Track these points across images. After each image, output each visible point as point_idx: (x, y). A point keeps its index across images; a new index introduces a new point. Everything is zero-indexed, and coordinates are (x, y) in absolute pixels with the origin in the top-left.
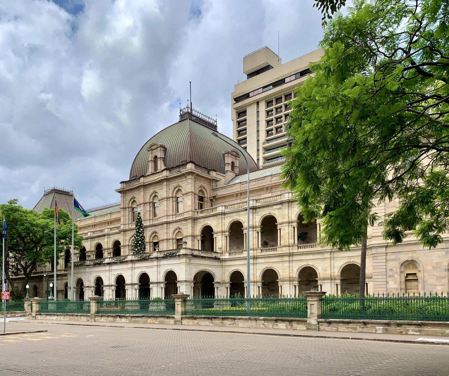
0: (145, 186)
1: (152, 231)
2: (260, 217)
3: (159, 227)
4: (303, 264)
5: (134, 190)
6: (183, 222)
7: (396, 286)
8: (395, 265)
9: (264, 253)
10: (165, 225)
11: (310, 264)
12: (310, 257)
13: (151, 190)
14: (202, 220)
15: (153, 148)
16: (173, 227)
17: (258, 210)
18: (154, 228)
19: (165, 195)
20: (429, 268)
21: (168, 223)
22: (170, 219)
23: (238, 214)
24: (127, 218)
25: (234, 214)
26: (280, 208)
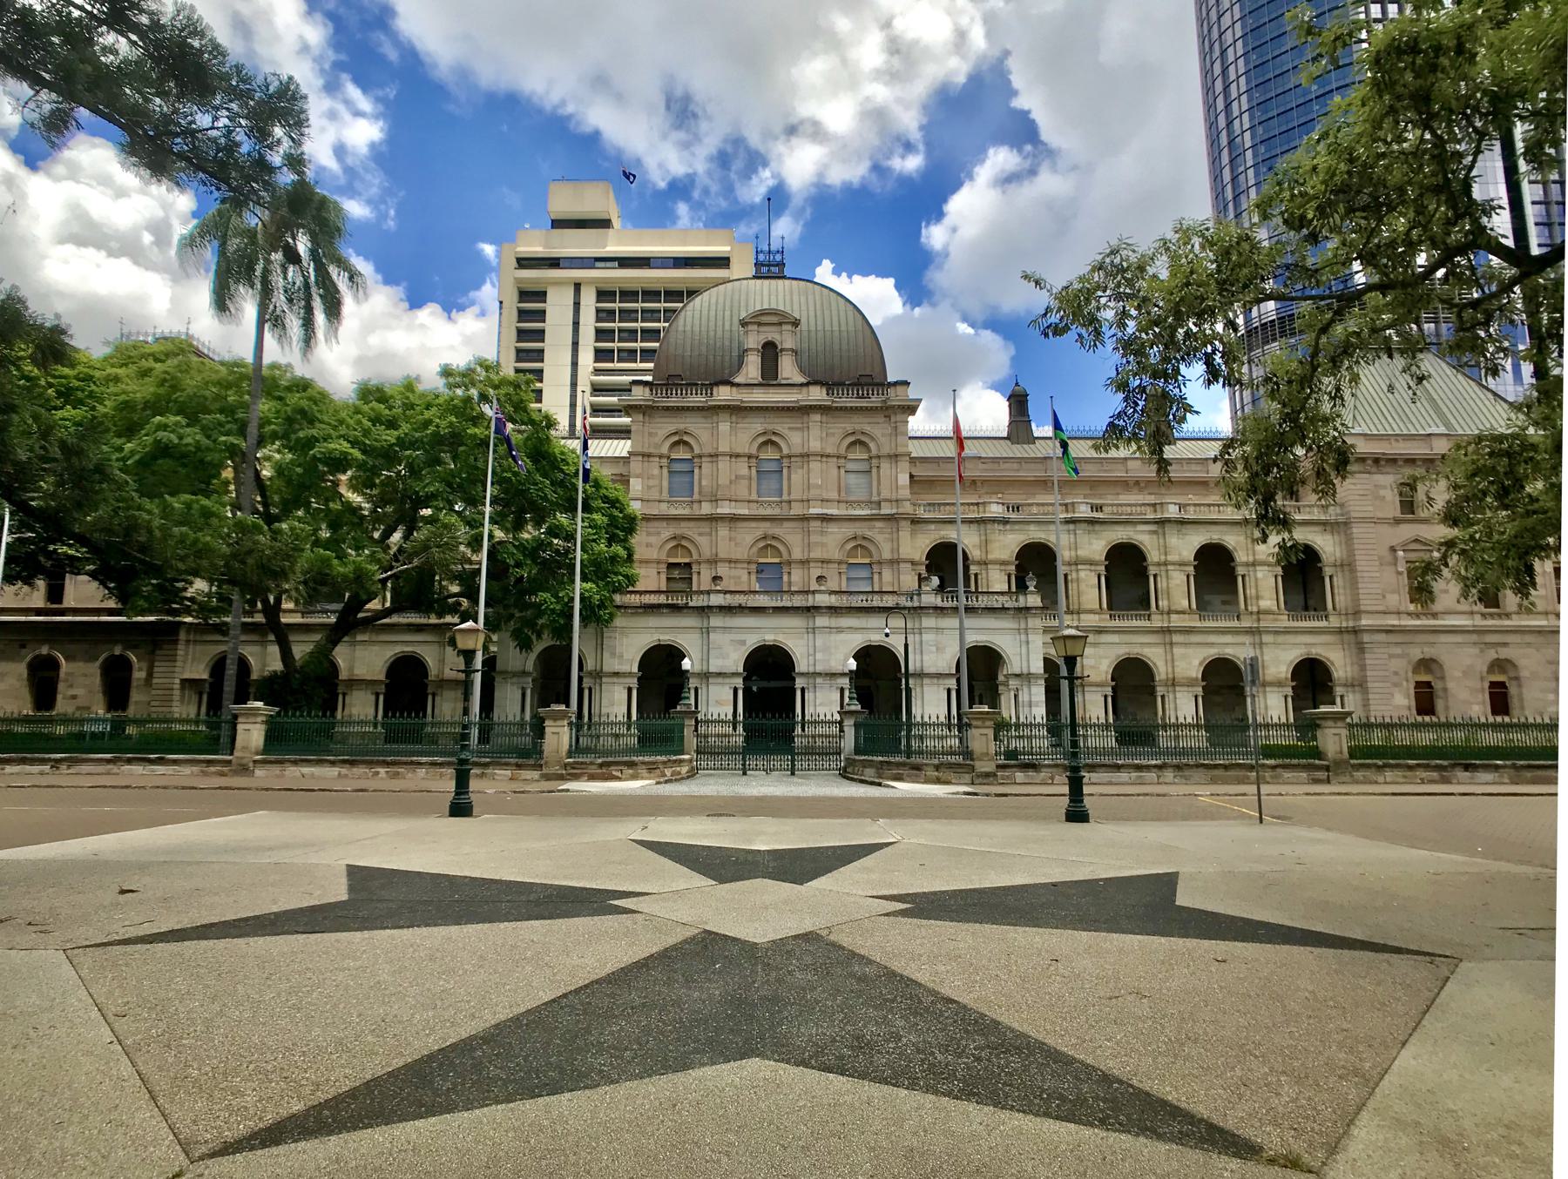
0: (737, 410)
1: (759, 533)
2: (1103, 543)
3: (786, 524)
4: (1213, 653)
5: (688, 414)
6: (879, 524)
7: (1405, 702)
8: (1401, 665)
9: (1117, 623)
10: (818, 523)
11: (1229, 652)
12: (1228, 639)
13: (757, 425)
14: (933, 527)
15: (765, 319)
16: (838, 533)
17: (1097, 527)
18: (768, 524)
19: (815, 445)
20: (1458, 674)
21: (825, 519)
22: (833, 511)
23: (1044, 527)
24: (656, 482)
25: (1032, 527)
26: (1155, 532)
